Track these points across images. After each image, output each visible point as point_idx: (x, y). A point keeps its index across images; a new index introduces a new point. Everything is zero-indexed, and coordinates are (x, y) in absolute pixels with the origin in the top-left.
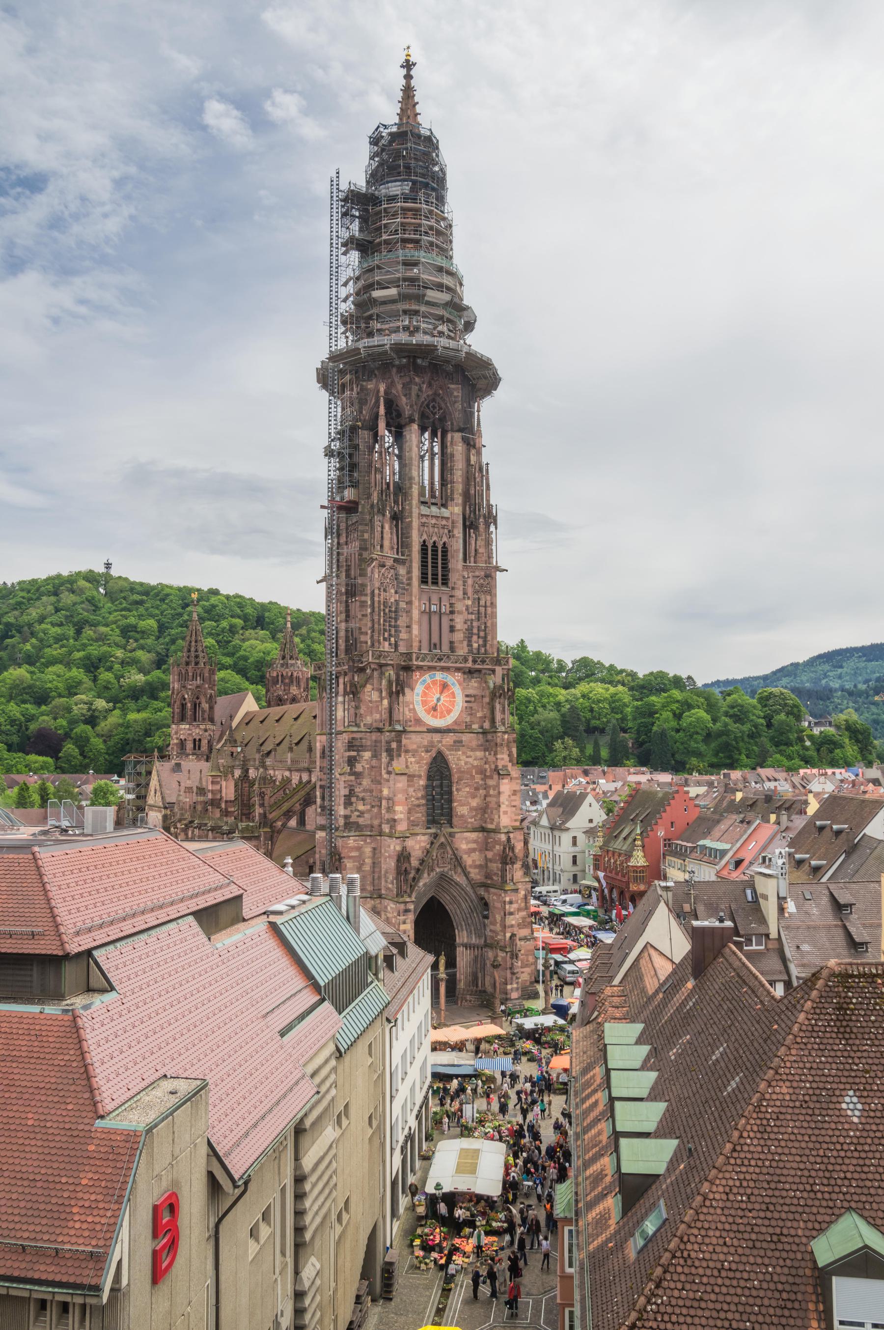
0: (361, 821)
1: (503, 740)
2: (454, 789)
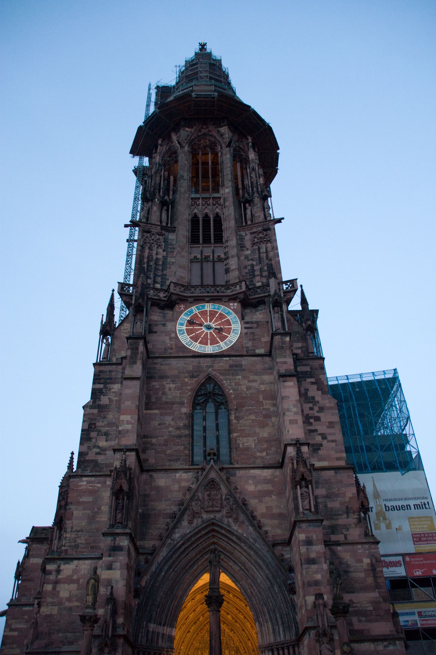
0: (101, 459)
1: (284, 342)
2: (233, 417)
